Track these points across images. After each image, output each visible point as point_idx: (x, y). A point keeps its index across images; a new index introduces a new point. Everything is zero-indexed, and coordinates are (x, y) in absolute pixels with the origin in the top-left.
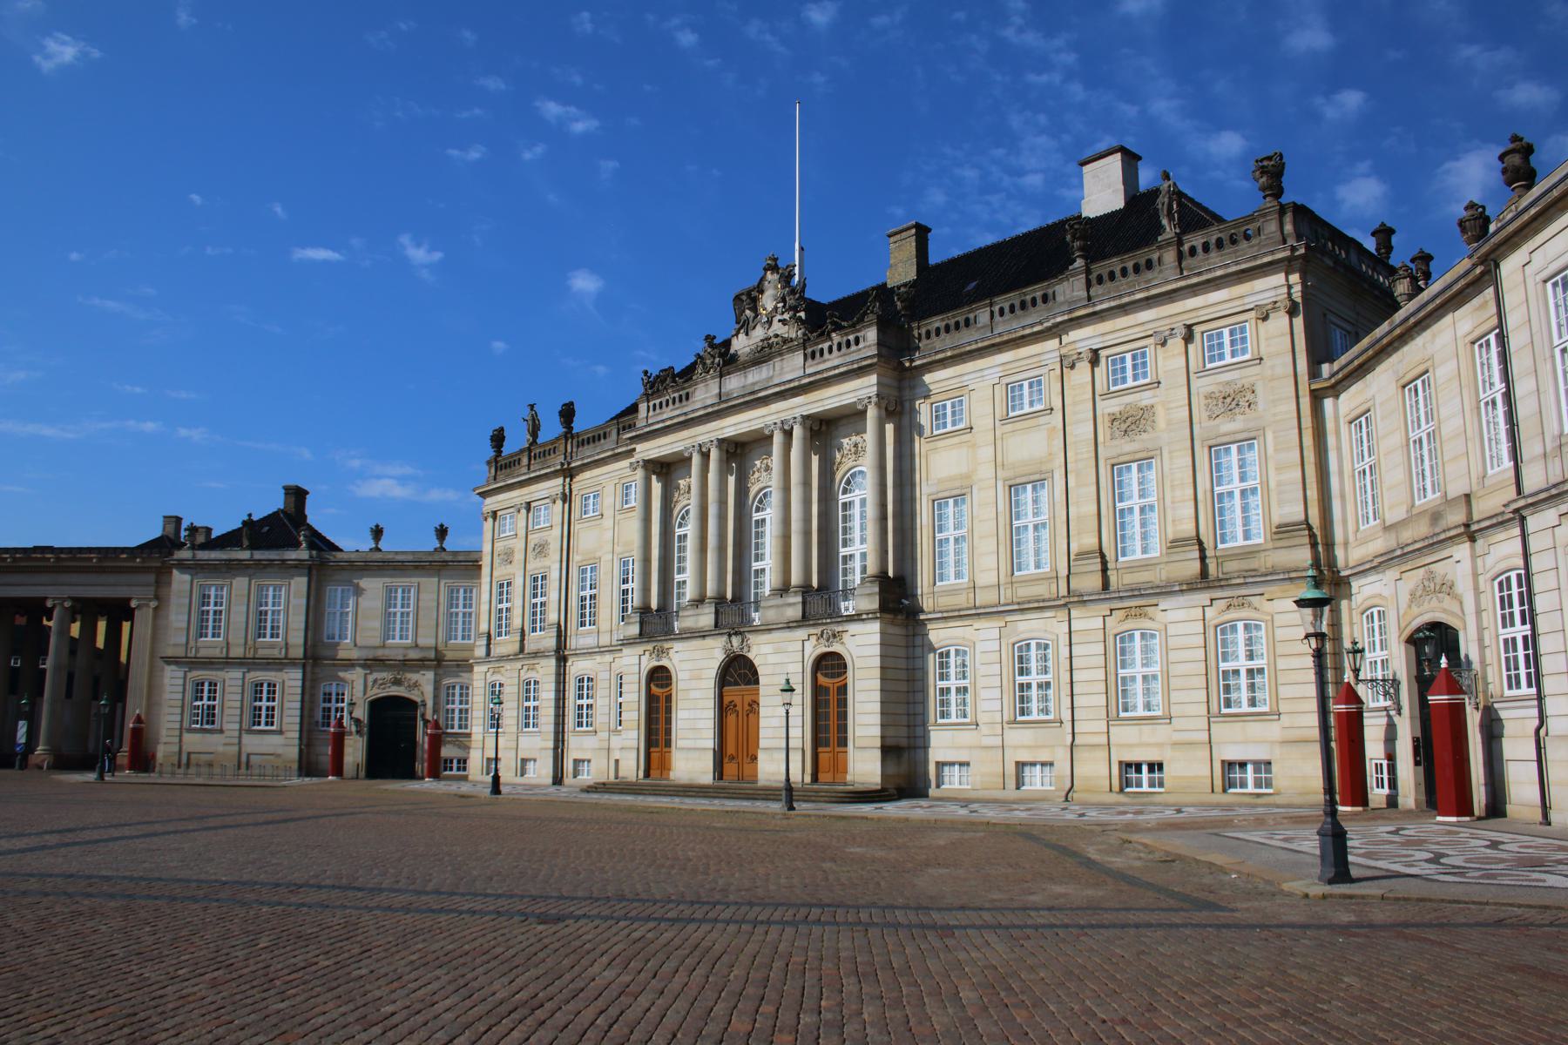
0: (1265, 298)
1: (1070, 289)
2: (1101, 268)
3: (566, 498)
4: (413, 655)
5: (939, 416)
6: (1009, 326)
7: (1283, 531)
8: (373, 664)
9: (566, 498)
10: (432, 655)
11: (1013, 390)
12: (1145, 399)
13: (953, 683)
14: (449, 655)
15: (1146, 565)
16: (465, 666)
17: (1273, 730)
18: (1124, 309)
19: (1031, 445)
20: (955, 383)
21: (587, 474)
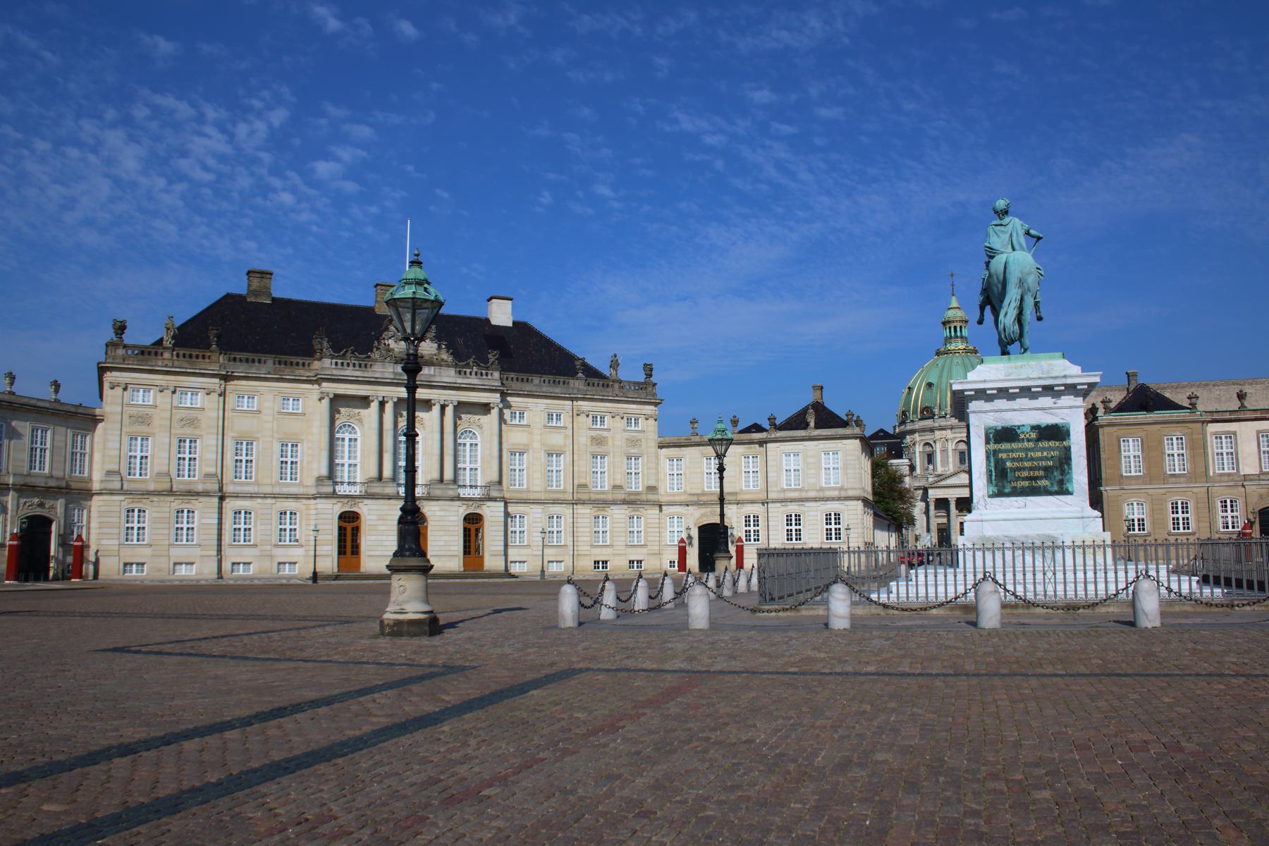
0: (649, 412)
1: (578, 384)
2: (591, 380)
3: (223, 394)
4: (52, 483)
5: (513, 415)
6: (546, 389)
7: (652, 489)
8: (25, 489)
9: (223, 394)
10: (64, 484)
11: (550, 416)
12: (605, 434)
13: (518, 529)
14: (73, 485)
15: (603, 493)
16: (88, 494)
17: (644, 550)
18: (602, 400)
19: (557, 439)
20: (523, 405)
21: (235, 382)
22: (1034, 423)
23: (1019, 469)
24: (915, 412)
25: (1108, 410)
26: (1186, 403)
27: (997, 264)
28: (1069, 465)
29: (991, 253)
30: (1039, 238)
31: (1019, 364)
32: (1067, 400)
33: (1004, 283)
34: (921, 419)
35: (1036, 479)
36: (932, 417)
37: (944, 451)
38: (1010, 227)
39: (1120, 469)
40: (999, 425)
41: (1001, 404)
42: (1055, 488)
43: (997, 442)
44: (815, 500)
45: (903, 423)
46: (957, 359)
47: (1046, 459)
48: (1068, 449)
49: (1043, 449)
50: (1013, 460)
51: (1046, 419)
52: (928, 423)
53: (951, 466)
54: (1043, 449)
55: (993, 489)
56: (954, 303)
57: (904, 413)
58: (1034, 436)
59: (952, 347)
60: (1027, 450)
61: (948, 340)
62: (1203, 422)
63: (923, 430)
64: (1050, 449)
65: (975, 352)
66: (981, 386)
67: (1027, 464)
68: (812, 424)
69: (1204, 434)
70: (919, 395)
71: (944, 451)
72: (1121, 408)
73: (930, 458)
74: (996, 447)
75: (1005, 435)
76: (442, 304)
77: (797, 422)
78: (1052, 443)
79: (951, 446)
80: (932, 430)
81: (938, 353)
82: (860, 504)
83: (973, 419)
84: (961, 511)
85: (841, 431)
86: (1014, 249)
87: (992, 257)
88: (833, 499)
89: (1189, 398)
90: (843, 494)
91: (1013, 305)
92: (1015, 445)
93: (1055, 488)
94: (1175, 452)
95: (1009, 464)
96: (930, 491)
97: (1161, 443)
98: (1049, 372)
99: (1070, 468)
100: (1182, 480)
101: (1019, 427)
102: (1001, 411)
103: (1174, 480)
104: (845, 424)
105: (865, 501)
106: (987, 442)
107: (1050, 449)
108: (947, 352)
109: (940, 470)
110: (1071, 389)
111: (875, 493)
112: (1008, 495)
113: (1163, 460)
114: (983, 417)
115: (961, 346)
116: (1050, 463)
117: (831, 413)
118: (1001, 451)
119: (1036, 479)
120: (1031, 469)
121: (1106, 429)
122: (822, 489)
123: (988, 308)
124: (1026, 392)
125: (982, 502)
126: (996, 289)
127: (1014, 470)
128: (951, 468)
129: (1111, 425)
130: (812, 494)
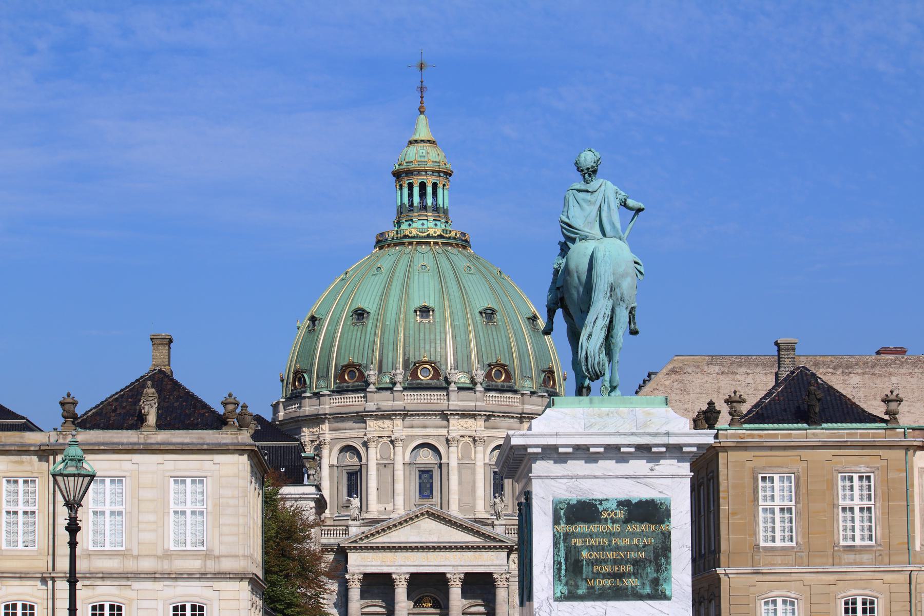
22: (623, 497)
23: (598, 562)
24: (323, 375)
25: (737, 419)
26: (879, 410)
27: (580, 253)
28: (668, 558)
29: (569, 238)
30: (639, 210)
31: (605, 410)
32: (669, 466)
33: (589, 287)
34: (338, 391)
35: (620, 576)
36: (362, 386)
37: (387, 466)
38: (599, 196)
39: (755, 534)
40: (574, 497)
41: (577, 466)
42: (648, 590)
43: (569, 521)
44: (153, 576)
45: (295, 397)
46: (423, 257)
47: (637, 548)
48: (667, 536)
49: (633, 534)
50: (591, 548)
51: (639, 493)
52: (353, 402)
53: (400, 500)
54: (633, 534)
55: (562, 589)
56: (423, 131)
57: (298, 376)
58: (621, 515)
59: (414, 228)
60: (612, 535)
61: (404, 213)
62: (907, 448)
63: (339, 417)
64: (642, 534)
65: (464, 244)
66: (552, 441)
67: (610, 555)
68: (152, 419)
69: (908, 470)
70: (339, 342)
71: (387, 466)
72: (763, 414)
73: (354, 482)
74: (569, 528)
75: (581, 512)
76: (75, 404)
77: (119, 413)
78: (645, 527)
79: (402, 455)
80: (361, 418)
81: (382, 243)
82: (245, 586)
83: (537, 488)
84: (418, 603)
85: (210, 436)
86: (604, 234)
87: (573, 241)
88: (190, 576)
89: (886, 401)
90: (211, 566)
91: (602, 323)
92: (594, 528)
93: (648, 590)
94: (857, 503)
95: (585, 554)
96: (354, 559)
97: (832, 485)
98: (645, 425)
99: (668, 563)
100: (866, 557)
101: (601, 501)
102: (577, 477)
103: (850, 557)
104: (218, 422)
105: (253, 581)
106: (556, 521)
107: (642, 534)
108: (402, 241)
109: (375, 509)
110: (675, 451)
111: (267, 571)
112: (582, 598)
113: (833, 519)
114: (550, 486)
115: (433, 227)
116: (642, 555)
117: (189, 397)
118: (574, 535)
119: (620, 576)
120: (615, 562)
121: (733, 455)
122: (167, 555)
123: (559, 312)
124: (613, 452)
125: (545, 607)
126: (576, 293)
127: (593, 563)
128: (400, 508)
129: (742, 447)
130: (147, 565)
